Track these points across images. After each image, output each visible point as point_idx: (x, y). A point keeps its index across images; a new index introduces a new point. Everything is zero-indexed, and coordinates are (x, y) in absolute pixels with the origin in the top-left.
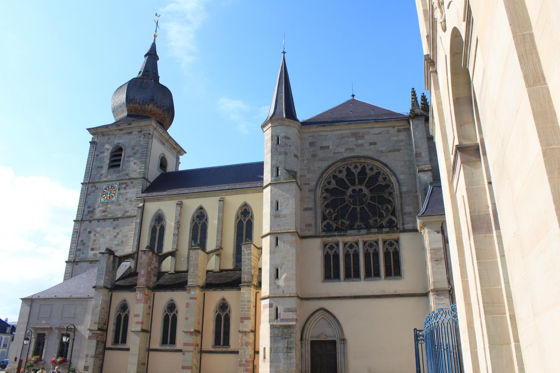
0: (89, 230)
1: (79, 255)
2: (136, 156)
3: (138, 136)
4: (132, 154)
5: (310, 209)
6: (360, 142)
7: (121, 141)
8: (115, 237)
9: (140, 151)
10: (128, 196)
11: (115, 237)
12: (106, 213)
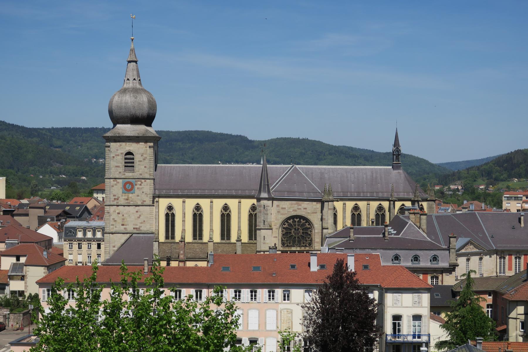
0: (117, 211)
1: (113, 228)
2: (145, 161)
3: (145, 146)
4: (142, 159)
5: (276, 237)
6: (300, 207)
8: (139, 217)
9: (148, 158)
10: (144, 190)
11: (139, 217)
12: (129, 201)
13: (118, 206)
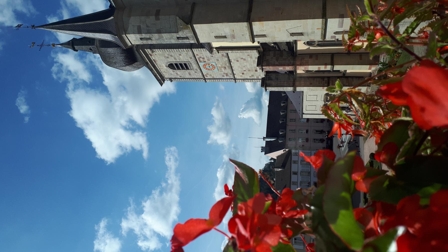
0: (241, 74)
2: (173, 55)
7: (164, 65)
8: (245, 60)
9: (168, 53)
11: (245, 60)
13: (234, 75)
